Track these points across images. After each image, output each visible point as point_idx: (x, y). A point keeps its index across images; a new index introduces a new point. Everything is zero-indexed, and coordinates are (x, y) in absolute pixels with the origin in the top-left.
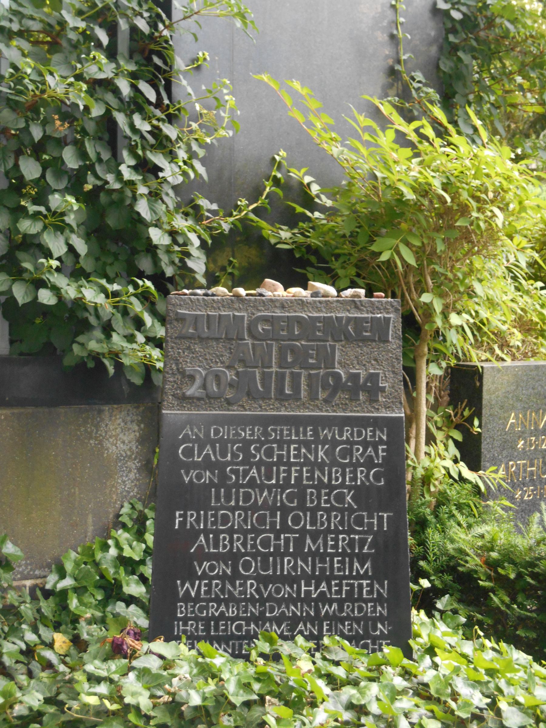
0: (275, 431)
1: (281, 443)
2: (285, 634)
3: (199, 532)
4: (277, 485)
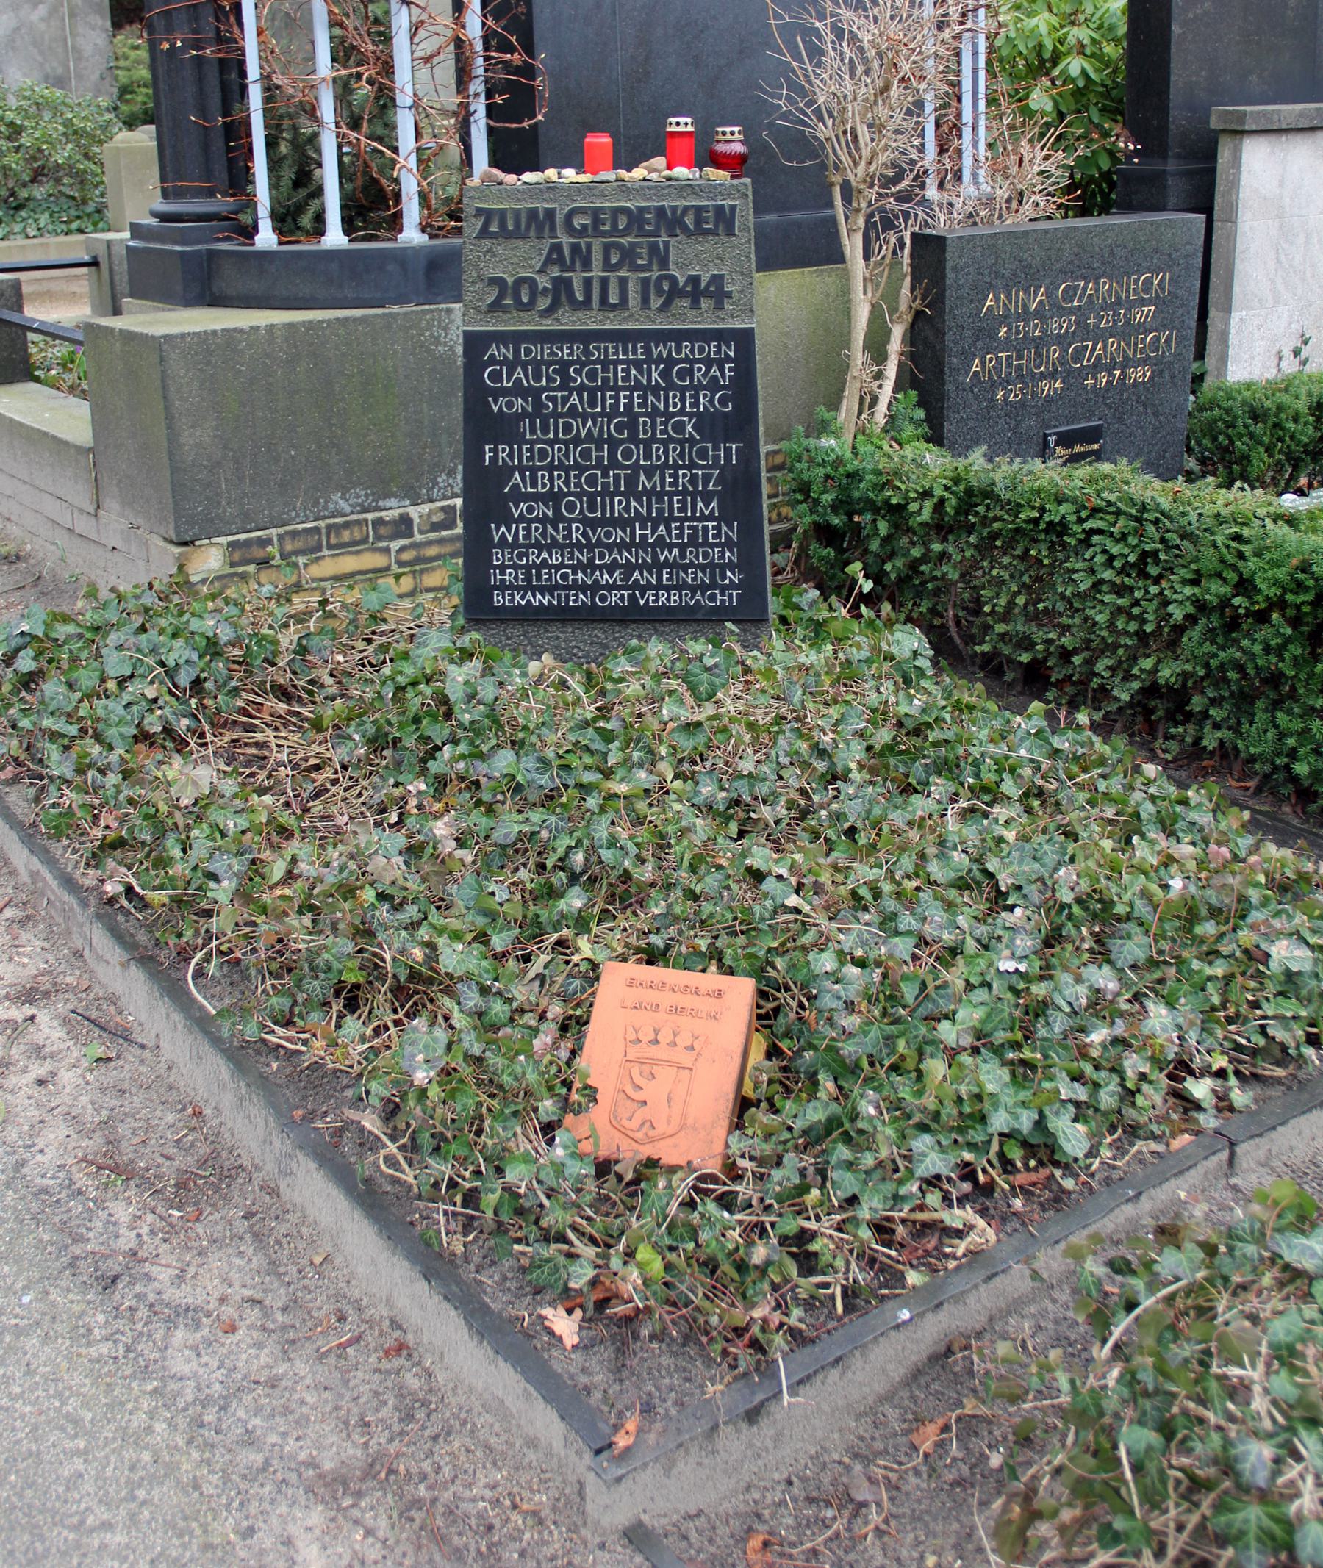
0: (598, 349)
1: (605, 364)
3: (513, 469)
4: (603, 414)
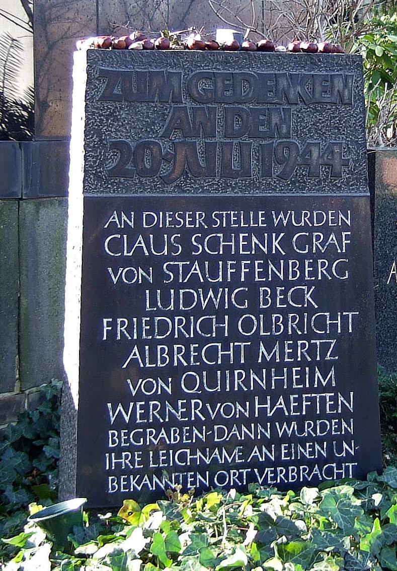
0: (220, 217)
1: (228, 232)
2: (238, 461)
3: (132, 343)
4: (224, 284)
